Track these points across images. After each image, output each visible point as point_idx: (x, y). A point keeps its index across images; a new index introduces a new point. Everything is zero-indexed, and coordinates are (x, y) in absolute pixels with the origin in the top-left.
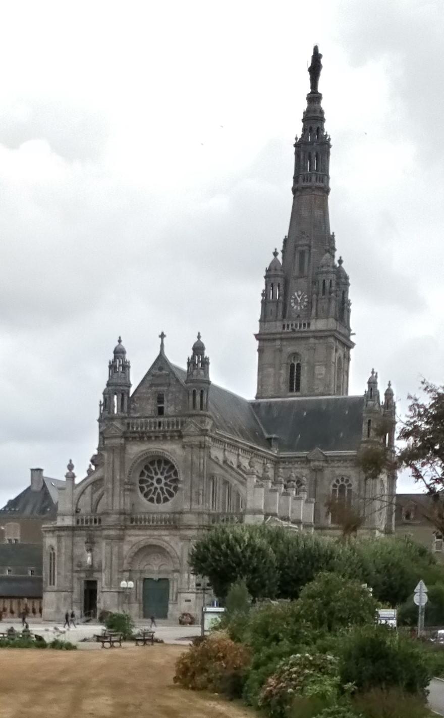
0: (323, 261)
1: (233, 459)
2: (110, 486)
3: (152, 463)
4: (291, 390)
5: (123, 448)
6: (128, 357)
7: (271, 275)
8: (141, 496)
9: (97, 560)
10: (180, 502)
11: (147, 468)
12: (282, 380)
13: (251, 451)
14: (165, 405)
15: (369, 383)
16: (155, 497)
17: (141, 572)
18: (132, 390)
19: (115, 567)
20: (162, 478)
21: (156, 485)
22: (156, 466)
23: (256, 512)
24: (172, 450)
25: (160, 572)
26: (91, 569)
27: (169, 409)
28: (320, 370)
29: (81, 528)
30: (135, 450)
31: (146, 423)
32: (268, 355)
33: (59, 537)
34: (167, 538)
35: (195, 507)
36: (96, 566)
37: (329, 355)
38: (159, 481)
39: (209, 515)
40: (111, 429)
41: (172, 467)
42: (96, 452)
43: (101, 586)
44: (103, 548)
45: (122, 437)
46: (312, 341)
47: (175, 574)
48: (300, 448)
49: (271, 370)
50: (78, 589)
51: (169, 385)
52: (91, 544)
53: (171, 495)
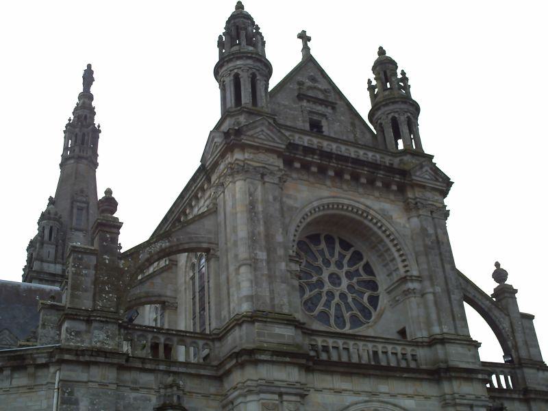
2: (262, 255)
3: (315, 239)
16: (332, 311)
20: (342, 274)
21: (328, 286)
22: (323, 245)
38: (335, 280)
40: (258, 129)
45: (279, 154)
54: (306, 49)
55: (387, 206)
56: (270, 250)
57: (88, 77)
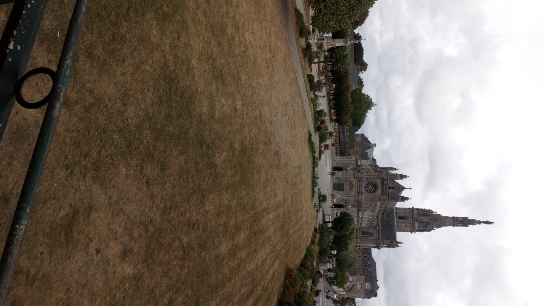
0: (434, 226)
1: (377, 210)
3: (375, 186)
4: (398, 217)
5: (379, 178)
6: (404, 179)
7: (430, 211)
8: (366, 183)
9: (349, 171)
10: (365, 194)
11: (374, 184)
12: (401, 214)
13: (380, 211)
14: (392, 189)
15: (400, 242)
17: (346, 183)
18: (395, 180)
19: (347, 176)
21: (369, 187)
23: (363, 214)
24: (379, 192)
25: (346, 188)
26: (346, 169)
27: (390, 191)
28: (404, 225)
29: (357, 166)
30: (379, 182)
31: (386, 184)
32: (408, 211)
33: (355, 160)
34: (355, 190)
35: (364, 198)
36: (347, 171)
37: (408, 227)
38: (370, 188)
39: (362, 202)
41: (374, 191)
42: (379, 166)
43: (342, 172)
44: (352, 173)
46: (412, 223)
47: (345, 193)
48: (382, 223)
49: (404, 211)
50: (341, 166)
51: (397, 190)
52: (353, 169)
53: (367, 191)
54: (408, 188)
55: (380, 192)
56: (370, 175)
57: (487, 223)
